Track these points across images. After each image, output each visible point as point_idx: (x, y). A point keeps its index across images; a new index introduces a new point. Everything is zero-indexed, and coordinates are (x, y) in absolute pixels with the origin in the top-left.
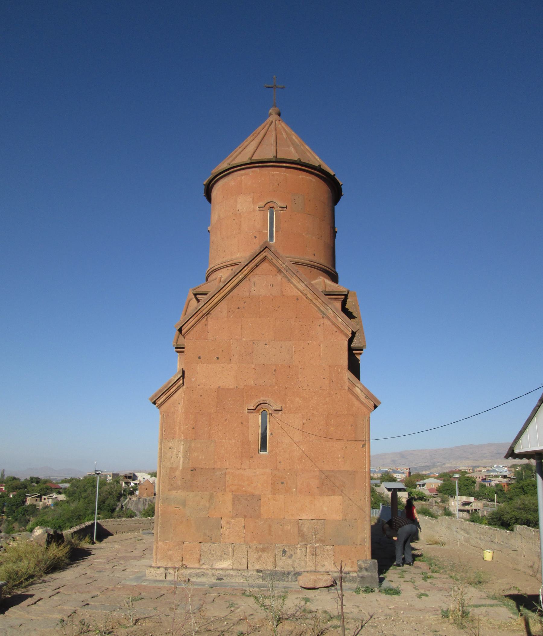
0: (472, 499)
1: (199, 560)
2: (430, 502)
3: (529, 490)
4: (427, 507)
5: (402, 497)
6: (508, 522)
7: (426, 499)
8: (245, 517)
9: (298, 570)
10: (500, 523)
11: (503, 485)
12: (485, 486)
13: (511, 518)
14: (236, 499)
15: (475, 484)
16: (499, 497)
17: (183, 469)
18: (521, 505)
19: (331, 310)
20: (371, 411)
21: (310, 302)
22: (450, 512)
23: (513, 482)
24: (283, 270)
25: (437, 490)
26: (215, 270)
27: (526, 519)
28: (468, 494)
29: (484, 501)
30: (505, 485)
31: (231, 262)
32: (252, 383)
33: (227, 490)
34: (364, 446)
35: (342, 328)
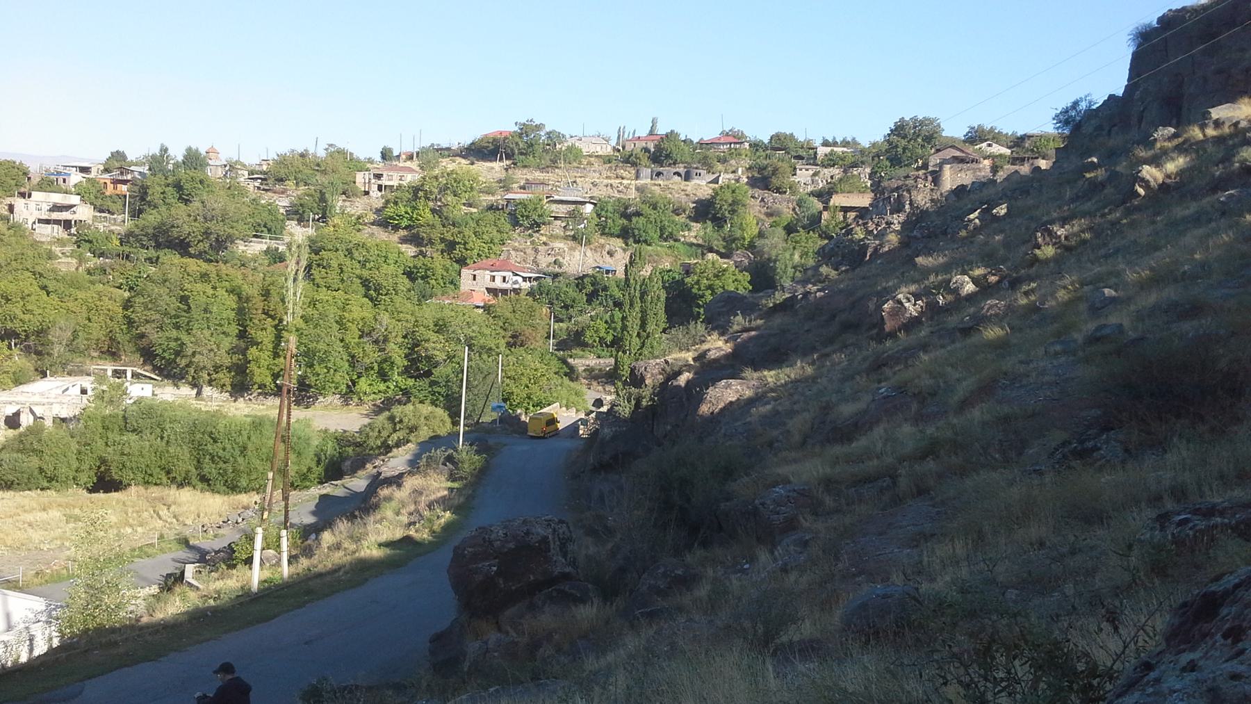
11: (103, 181)
30: (108, 182)
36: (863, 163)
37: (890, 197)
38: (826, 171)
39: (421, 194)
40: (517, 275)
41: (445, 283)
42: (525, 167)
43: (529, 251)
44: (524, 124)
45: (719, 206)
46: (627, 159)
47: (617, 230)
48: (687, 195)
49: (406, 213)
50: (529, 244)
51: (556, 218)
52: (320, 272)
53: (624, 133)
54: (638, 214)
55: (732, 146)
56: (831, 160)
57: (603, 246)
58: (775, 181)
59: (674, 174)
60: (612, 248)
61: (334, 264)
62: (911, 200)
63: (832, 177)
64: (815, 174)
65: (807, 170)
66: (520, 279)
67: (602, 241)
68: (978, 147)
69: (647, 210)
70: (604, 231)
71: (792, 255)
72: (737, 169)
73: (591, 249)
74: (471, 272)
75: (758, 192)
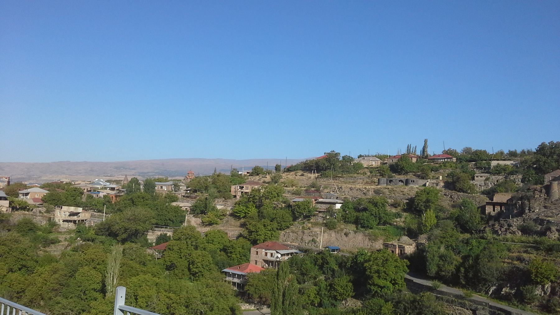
0: (80, 210)
2: (34, 212)
4: (31, 217)
5: (2, 206)
6: (117, 233)
7: (29, 209)
10: (107, 233)
11: (111, 196)
12: (93, 197)
13: (120, 229)
15: (82, 195)
16: (107, 208)
18: (132, 216)
22: (55, 222)
23: (123, 194)
25: (42, 200)
27: (135, 230)
28: (74, 204)
29: (91, 212)
30: (114, 196)
36: (517, 172)
37: (516, 204)
38: (493, 177)
39: (251, 199)
40: (277, 252)
41: (241, 257)
42: (327, 177)
43: (300, 233)
44: (329, 154)
45: (416, 203)
46: (380, 172)
47: (353, 219)
48: (404, 194)
49: (243, 210)
50: (301, 228)
51: (320, 212)
52: (168, 253)
53: (410, 148)
54: (365, 209)
55: (446, 160)
56: (497, 170)
57: (342, 230)
58: (458, 185)
59: (399, 181)
60: (348, 231)
61: (176, 248)
62: (529, 207)
63: (497, 181)
64: (487, 179)
65: (481, 177)
66: (279, 256)
67: (343, 226)
69: (371, 207)
70: (346, 220)
71: (439, 248)
72: (439, 177)
73: (335, 232)
74: (255, 249)
75: (449, 192)
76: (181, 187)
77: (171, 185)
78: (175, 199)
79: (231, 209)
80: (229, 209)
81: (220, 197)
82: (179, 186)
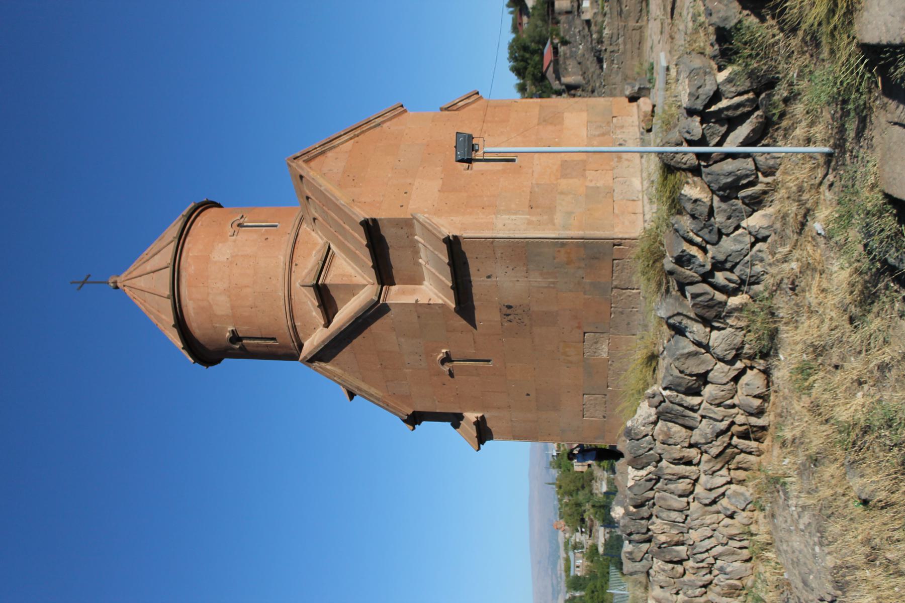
1: (634, 200)
3: (598, 598)
8: (584, 170)
9: (638, 135)
14: (564, 176)
17: (529, 215)
19: (376, 118)
20: (481, 98)
21: (362, 135)
24: (323, 149)
26: (290, 295)
31: (288, 264)
32: (439, 169)
33: (555, 182)
34: (515, 102)
35: (397, 113)
68: (531, 11)
76: (578, 540)
77: (574, 553)
78: (594, 549)
79: (607, 472)
80: (606, 474)
81: (591, 486)
82: (576, 543)
